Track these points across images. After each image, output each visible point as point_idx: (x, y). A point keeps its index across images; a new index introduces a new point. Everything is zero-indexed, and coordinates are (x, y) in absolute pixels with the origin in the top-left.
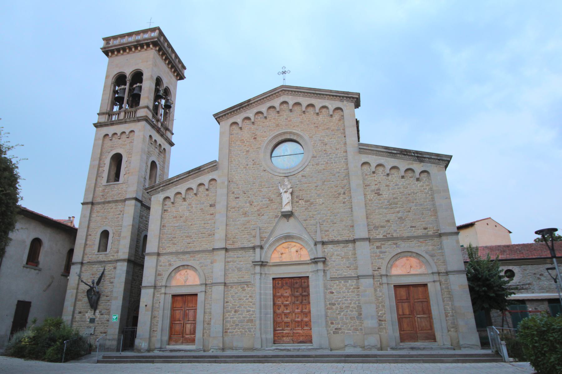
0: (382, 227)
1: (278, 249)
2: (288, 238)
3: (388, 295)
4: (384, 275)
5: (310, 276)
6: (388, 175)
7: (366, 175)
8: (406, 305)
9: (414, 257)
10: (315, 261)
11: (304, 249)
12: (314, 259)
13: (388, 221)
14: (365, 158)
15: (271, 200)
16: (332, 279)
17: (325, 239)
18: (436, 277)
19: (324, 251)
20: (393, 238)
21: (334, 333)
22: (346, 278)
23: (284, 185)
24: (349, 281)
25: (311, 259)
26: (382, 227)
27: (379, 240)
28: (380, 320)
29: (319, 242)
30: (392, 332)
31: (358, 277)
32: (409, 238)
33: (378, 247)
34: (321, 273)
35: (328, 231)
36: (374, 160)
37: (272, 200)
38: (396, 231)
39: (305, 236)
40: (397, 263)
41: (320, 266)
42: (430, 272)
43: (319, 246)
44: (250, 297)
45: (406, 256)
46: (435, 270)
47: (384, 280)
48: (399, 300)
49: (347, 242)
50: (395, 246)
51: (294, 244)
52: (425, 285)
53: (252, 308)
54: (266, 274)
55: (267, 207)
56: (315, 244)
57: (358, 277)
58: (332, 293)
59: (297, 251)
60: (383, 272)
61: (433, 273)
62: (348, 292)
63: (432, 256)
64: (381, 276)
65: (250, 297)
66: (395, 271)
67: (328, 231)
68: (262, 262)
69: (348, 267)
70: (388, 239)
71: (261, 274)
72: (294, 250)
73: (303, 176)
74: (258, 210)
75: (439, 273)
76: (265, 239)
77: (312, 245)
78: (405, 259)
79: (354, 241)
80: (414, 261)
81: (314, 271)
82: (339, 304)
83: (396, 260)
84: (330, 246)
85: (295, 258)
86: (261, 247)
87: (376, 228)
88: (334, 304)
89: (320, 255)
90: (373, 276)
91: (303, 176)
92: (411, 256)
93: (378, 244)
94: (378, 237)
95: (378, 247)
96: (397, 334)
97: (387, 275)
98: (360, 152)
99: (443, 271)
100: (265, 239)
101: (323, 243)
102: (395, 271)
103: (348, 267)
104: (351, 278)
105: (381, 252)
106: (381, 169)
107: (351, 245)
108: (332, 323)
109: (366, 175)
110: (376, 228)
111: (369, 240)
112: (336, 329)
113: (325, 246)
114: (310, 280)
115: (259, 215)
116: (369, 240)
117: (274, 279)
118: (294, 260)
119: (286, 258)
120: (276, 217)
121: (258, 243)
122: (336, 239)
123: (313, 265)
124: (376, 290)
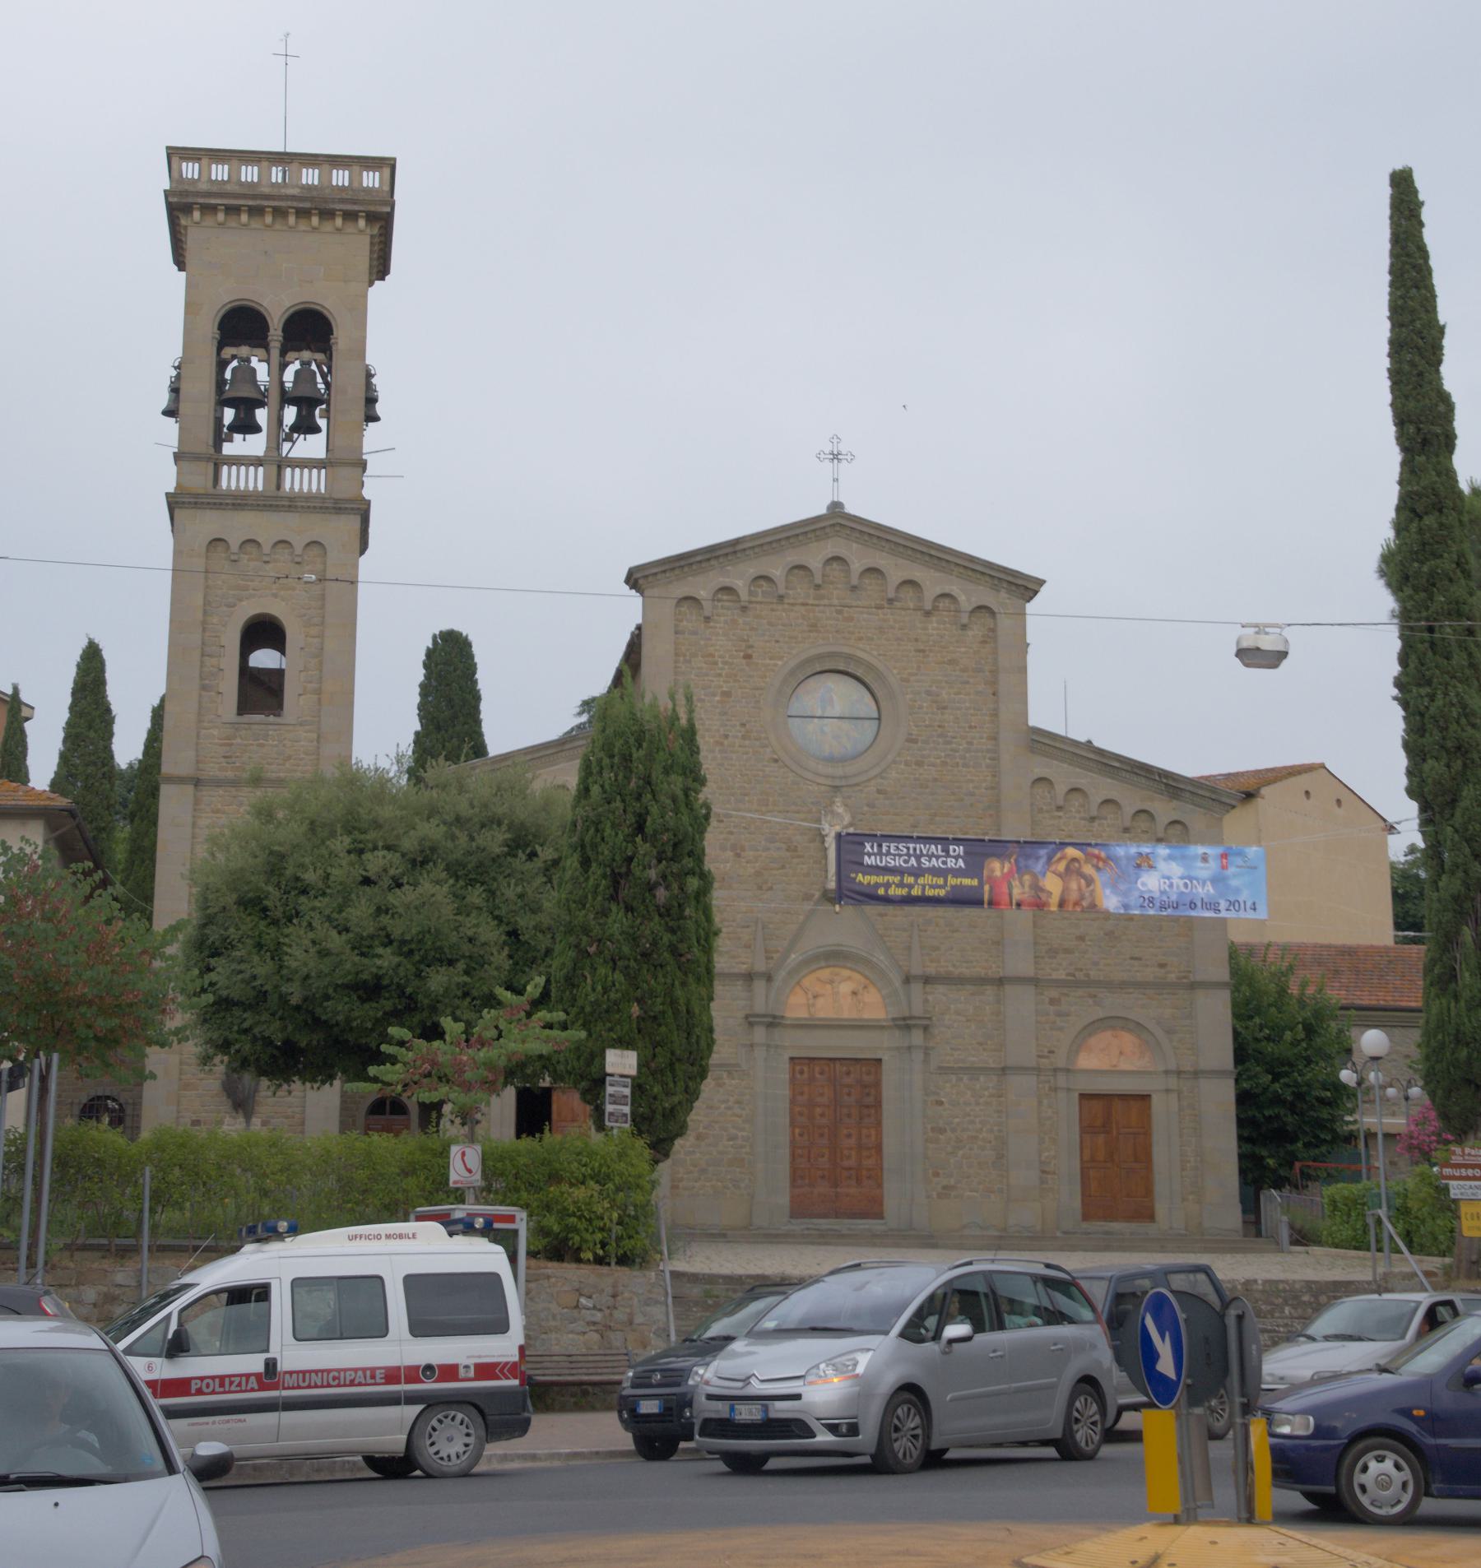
0: (1067, 951)
1: (806, 982)
2: (835, 957)
3: (1067, 1115)
4: (1061, 1070)
5: (885, 1058)
6: (1093, 819)
7: (1041, 810)
8: (1101, 1139)
9: (1130, 1031)
10: (904, 1024)
11: (872, 990)
12: (904, 1019)
13: (1081, 938)
14: (1040, 767)
15: (792, 849)
16: (943, 1070)
17: (931, 970)
18: (1173, 1082)
19: (926, 1001)
20: (1089, 983)
21: (939, 1196)
22: (974, 1071)
23: (832, 812)
24: (982, 1078)
25: (894, 1019)
26: (1067, 951)
27: (1058, 983)
28: (1043, 1172)
29: (915, 977)
30: (1069, 1196)
31: (1004, 1070)
32: (1123, 985)
33: (1052, 1001)
34: (918, 1056)
35: (937, 949)
36: (1063, 775)
37: (795, 850)
38: (1096, 964)
39: (880, 958)
40: (1093, 1041)
41: (917, 1037)
42: (1161, 1068)
43: (917, 988)
44: (738, 1102)
45: (1113, 1028)
46: (1172, 1066)
47: (1062, 1081)
48: (1087, 1129)
49: (982, 981)
50: (1091, 1001)
51: (846, 973)
52: (1145, 1098)
53: (742, 1130)
54: (777, 1047)
55: (783, 867)
56: (908, 980)
57: (1004, 1069)
58: (941, 1103)
59: (854, 993)
60: (1061, 1064)
61: (1167, 1072)
62: (978, 1104)
63: (1169, 1032)
64: (1055, 1070)
65: (738, 1102)
66: (1086, 1061)
67: (937, 949)
68: (774, 1017)
69: (980, 1044)
70: (1076, 984)
71: (768, 1046)
72: (845, 988)
73: (879, 792)
74: (758, 874)
75: (1179, 1073)
76: (776, 956)
77: (898, 983)
78: (1109, 1034)
79: (1001, 982)
80: (1128, 1040)
81: (898, 1048)
82: (953, 1130)
83: (1090, 1035)
84: (941, 988)
85: (847, 1011)
86: (769, 978)
87: (1053, 952)
88: (942, 1131)
89: (918, 1010)
90: (1038, 1070)
91: (879, 792)
92: (1123, 1028)
93: (1054, 993)
94: (1055, 976)
95: (1052, 1001)
96: (1077, 1203)
97: (1068, 1070)
98: (1032, 751)
99: (1189, 1068)
100: (776, 956)
101: (927, 980)
102: (1086, 1061)
103: (980, 1044)
104: (985, 1070)
105: (1059, 1014)
106: (1076, 800)
107: (990, 991)
108: (937, 1175)
109: (1041, 810)
110: (1053, 952)
111: (1035, 981)
112: (944, 1188)
113: (929, 988)
114: (885, 1066)
115: (760, 888)
116: (1035, 981)
117: (792, 1059)
118: (846, 1015)
119: (824, 1010)
120: (807, 897)
121: (761, 966)
122: (957, 972)
123: (897, 1033)
124: (1040, 1103)
